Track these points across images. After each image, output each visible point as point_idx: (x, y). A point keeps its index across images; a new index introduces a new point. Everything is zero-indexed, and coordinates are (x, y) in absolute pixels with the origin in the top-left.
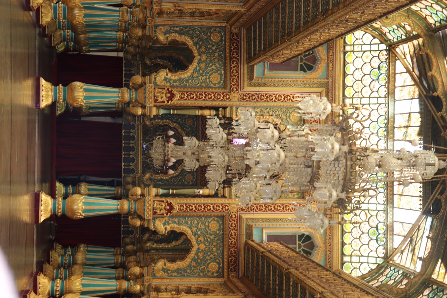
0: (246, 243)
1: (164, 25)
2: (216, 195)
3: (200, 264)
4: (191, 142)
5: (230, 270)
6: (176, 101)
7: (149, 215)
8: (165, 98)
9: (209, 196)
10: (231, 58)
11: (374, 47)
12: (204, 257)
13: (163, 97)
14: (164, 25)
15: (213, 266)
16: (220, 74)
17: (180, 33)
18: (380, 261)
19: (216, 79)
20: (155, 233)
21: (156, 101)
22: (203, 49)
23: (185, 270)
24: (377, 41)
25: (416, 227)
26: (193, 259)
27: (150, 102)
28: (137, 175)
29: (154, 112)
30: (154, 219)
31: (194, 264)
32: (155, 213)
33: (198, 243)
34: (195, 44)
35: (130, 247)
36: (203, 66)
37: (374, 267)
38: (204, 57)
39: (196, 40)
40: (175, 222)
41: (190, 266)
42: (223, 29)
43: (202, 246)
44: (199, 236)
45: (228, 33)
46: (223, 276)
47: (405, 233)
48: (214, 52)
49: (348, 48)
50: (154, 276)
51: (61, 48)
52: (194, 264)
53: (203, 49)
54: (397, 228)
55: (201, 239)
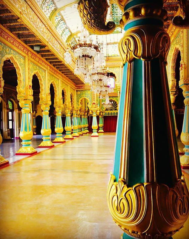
1: (77, 106)
8: (95, 105)
10: (84, 88)
13: (94, 106)
17: (78, 102)
19: (89, 92)
21: (95, 107)
22: (82, 96)
27: (96, 109)
29: (98, 108)
36: (86, 96)
38: (84, 95)
39: (80, 98)
45: (78, 89)
48: (83, 93)
53: (82, 96)
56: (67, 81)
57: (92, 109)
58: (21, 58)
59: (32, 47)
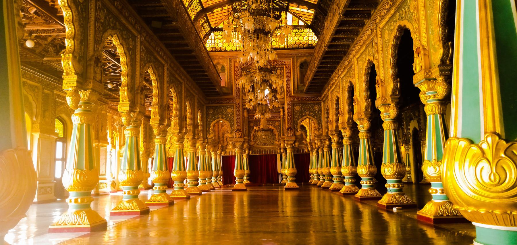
0: (305, 93)
2: (283, 108)
3: (315, 114)
4: (257, 116)
5: (318, 100)
6: (241, 128)
7: (294, 138)
9: (284, 112)
11: (213, 38)
12: (312, 112)
14: (207, 135)
15: (316, 108)
16: (228, 108)
17: (210, 127)
18: (311, 31)
19: (229, 111)
20: (301, 135)
21: (241, 137)
22: (216, 117)
23: (318, 121)
24: (210, 37)
25: (294, 14)
26: (313, 117)
28: (277, 147)
30: (295, 135)
31: (315, 117)
32: (293, 135)
33: (306, 115)
34: (214, 120)
35: (309, 149)
37: (314, 33)
38: (220, 116)
40: (297, 127)
41: (316, 119)
42: (208, 108)
43: (307, 113)
44: (302, 115)
46: (320, 104)
47: (297, 19)
49: (214, 50)
50: (322, 134)
51: (221, 184)
52: (315, 117)
54: (295, 24)
55: (304, 114)
56: (194, 89)
57: (234, 140)
58: (130, 39)
59: (148, 21)
